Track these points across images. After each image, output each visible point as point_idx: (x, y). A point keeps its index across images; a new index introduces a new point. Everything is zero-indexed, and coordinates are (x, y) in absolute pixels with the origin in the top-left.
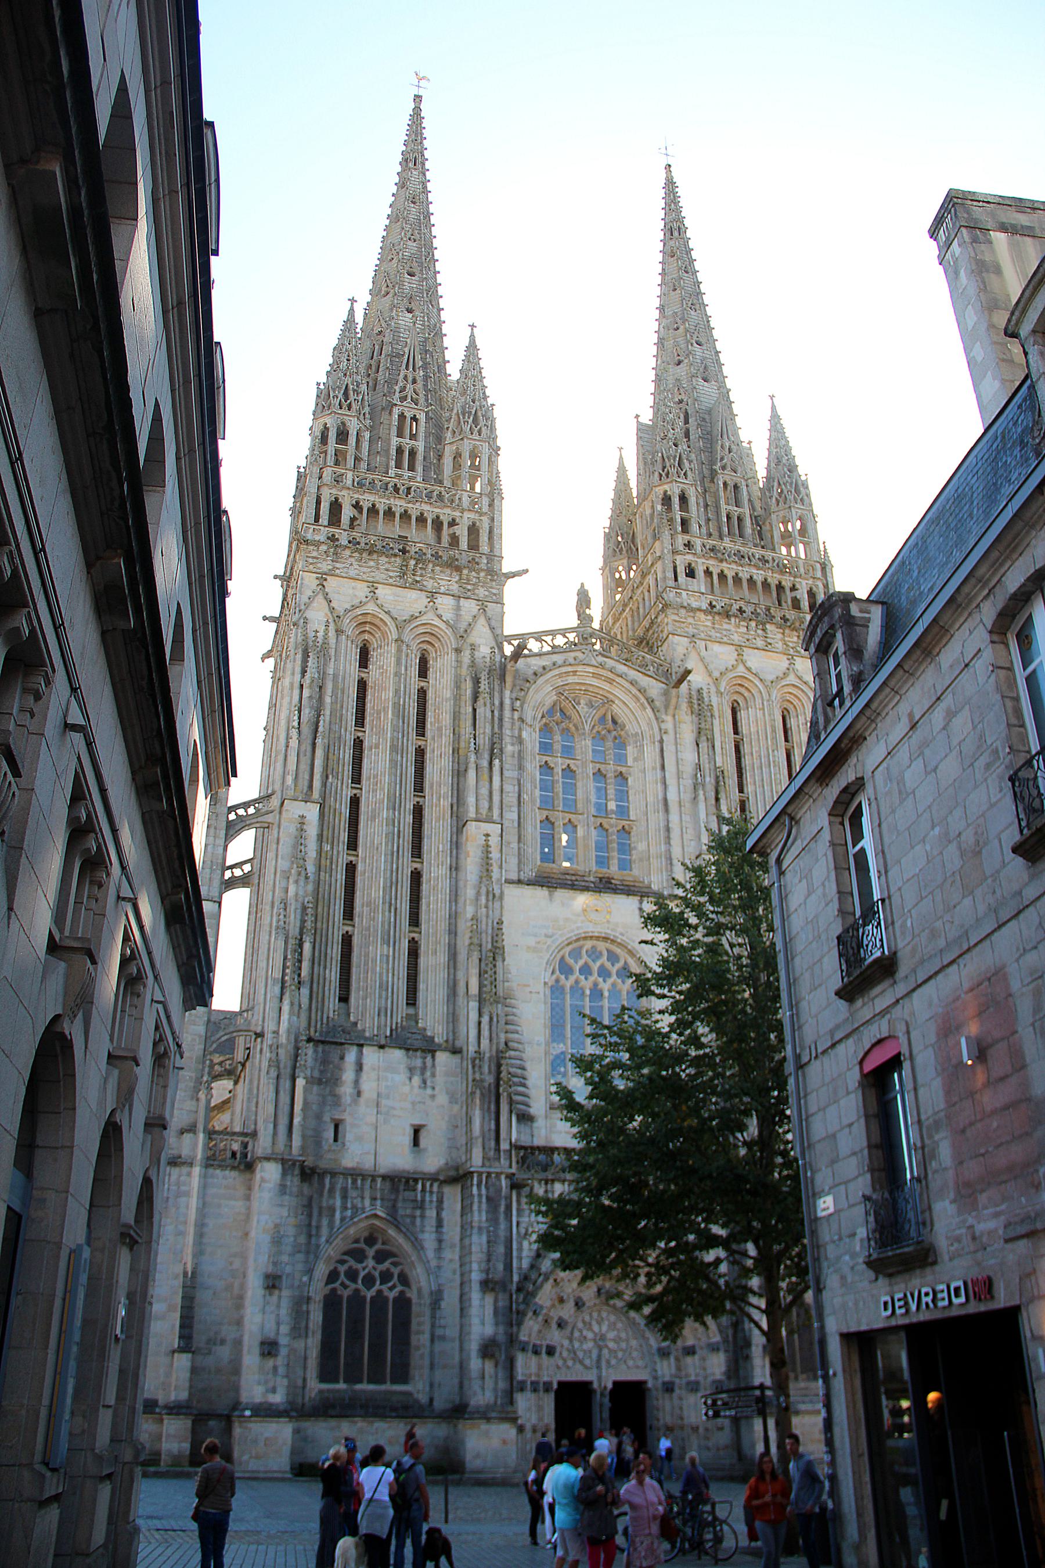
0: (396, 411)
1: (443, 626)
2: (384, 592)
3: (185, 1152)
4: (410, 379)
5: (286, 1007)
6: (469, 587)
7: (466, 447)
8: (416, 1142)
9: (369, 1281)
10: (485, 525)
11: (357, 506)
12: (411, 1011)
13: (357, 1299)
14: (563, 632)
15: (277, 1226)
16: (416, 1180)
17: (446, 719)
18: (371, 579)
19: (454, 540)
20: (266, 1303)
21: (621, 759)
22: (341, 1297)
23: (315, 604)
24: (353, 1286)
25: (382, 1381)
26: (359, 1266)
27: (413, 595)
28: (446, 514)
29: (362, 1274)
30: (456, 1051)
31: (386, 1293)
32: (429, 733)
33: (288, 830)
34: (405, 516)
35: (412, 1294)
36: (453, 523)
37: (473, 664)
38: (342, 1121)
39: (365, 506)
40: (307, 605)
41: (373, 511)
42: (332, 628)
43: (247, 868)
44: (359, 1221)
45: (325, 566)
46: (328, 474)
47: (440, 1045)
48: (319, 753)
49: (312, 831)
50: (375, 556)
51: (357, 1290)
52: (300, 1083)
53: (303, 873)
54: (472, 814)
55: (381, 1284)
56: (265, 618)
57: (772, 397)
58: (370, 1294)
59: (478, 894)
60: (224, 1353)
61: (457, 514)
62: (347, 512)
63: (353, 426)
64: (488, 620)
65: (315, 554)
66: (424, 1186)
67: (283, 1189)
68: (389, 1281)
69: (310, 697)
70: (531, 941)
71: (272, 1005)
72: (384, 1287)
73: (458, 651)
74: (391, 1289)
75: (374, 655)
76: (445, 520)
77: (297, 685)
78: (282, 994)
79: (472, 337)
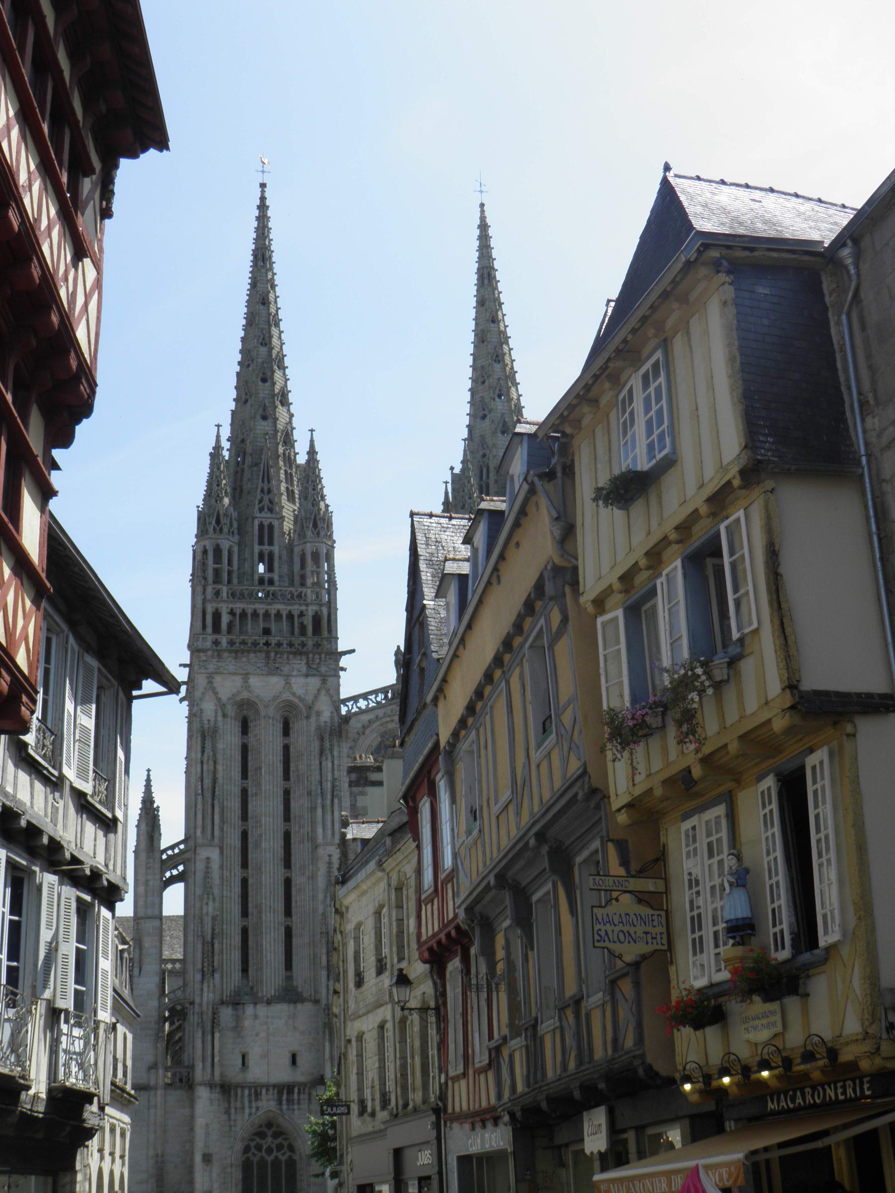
0: (256, 522)
2: (254, 681)
3: (152, 1083)
4: (266, 491)
5: (205, 989)
7: (309, 548)
9: (269, 1151)
10: (325, 611)
11: (232, 613)
12: (289, 974)
13: (262, 1163)
14: (384, 690)
15: (207, 1125)
16: (294, 1087)
18: (244, 672)
19: (303, 628)
23: (207, 697)
24: (259, 1154)
26: (263, 1142)
27: (274, 680)
28: (296, 609)
29: (265, 1147)
30: (317, 1002)
31: (280, 1157)
32: (292, 779)
33: (200, 866)
34: (267, 615)
35: (296, 1157)
36: (302, 614)
37: (318, 728)
39: (238, 612)
40: (201, 699)
41: (243, 614)
42: (220, 713)
45: (212, 667)
46: (210, 590)
48: (217, 810)
49: (215, 866)
50: (246, 654)
51: (262, 1158)
52: (217, 1035)
53: (211, 897)
54: (320, 840)
58: (270, 1159)
59: (325, 897)
61: (303, 608)
62: (225, 619)
63: (225, 545)
64: (328, 690)
65: (204, 658)
66: (299, 1089)
69: (208, 770)
71: (198, 986)
72: (279, 1155)
73: (308, 717)
74: (283, 1154)
75: (251, 724)
77: (199, 761)
78: (203, 979)
79: (312, 442)
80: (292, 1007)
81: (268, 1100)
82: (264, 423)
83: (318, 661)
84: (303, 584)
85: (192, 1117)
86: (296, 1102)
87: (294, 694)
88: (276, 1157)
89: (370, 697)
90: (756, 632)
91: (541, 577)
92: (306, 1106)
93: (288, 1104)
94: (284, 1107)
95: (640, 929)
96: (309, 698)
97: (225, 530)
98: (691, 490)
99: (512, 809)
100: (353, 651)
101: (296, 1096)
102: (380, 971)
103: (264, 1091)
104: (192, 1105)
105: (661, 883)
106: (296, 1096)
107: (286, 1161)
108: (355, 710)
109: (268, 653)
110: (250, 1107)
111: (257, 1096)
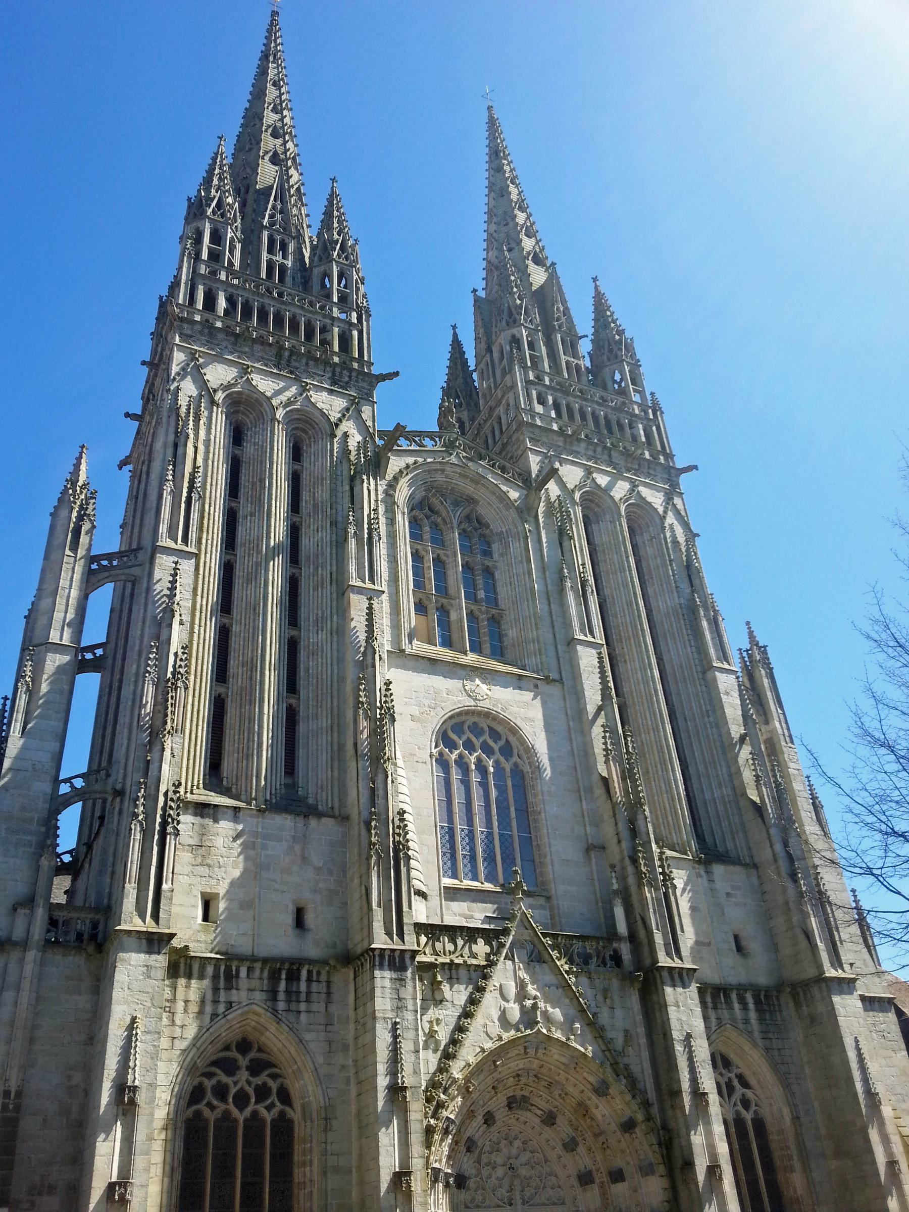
10: (355, 333)
11: (231, 300)
14: (431, 436)
21: (487, 553)
22: (207, 1121)
24: (222, 1106)
29: (233, 1091)
31: (263, 1112)
35: (295, 1115)
43: (99, 652)
51: (227, 1114)
55: (257, 1102)
56: (127, 415)
57: (595, 280)
58: (241, 1117)
65: (189, 332)
66: (310, 972)
68: (266, 1098)
70: (416, 711)
74: (269, 1108)
80: (300, 820)
81: (251, 990)
83: (347, 379)
86: (303, 996)
88: (255, 1113)
92: (323, 1005)
93: (288, 1001)
94: (281, 1005)
100: (396, 374)
101: (303, 987)
106: (303, 987)
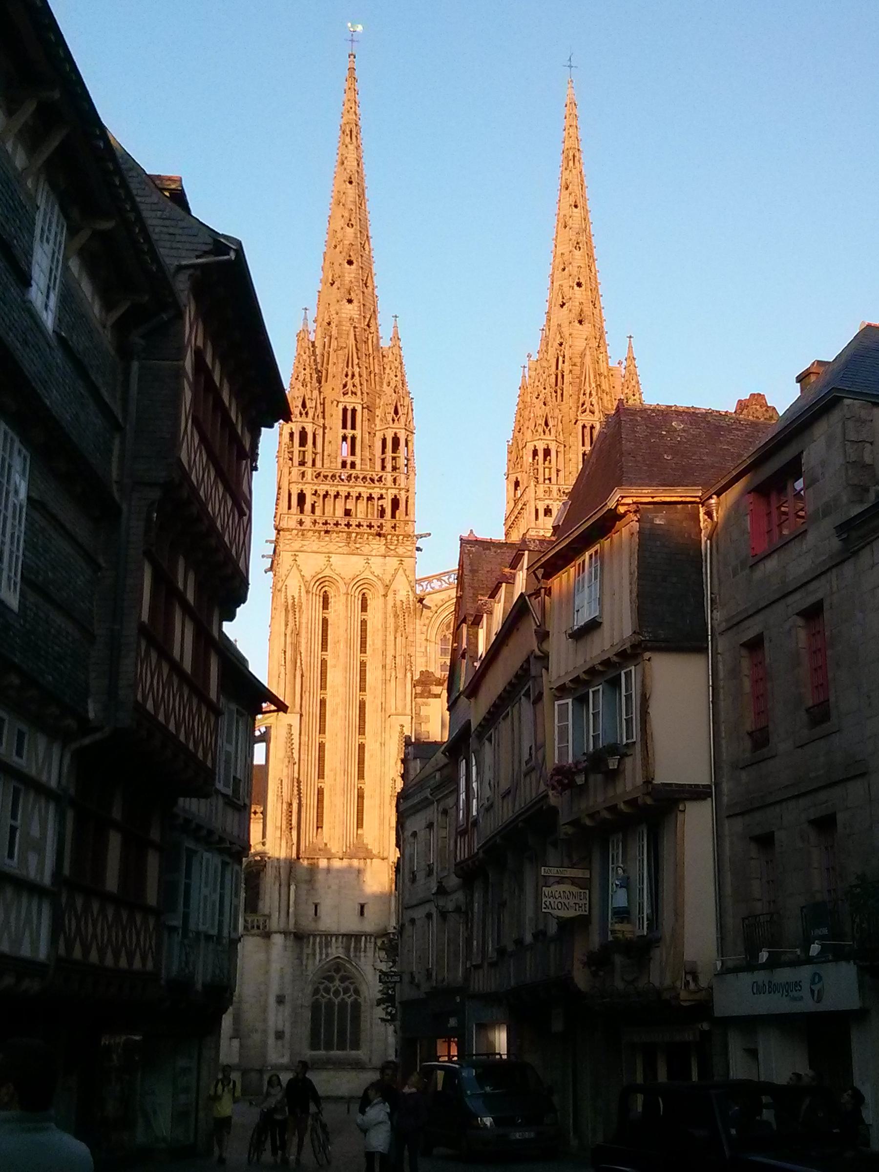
1: (375, 579)
6: (392, 547)
8: (362, 913)
15: (282, 968)
17: (379, 644)
18: (327, 551)
20: (277, 1011)
24: (329, 997)
25: (344, 1049)
26: (331, 985)
27: (354, 558)
36: (381, 497)
38: (318, 903)
40: (287, 576)
44: (331, 960)
45: (297, 545)
47: (374, 855)
49: (295, 731)
52: (293, 888)
55: (344, 994)
58: (336, 1001)
60: (257, 1037)
61: (384, 491)
65: (290, 537)
67: (285, 948)
72: (345, 997)
73: (385, 596)
74: (349, 997)
75: (331, 600)
76: (375, 496)
79: (395, 327)
82: (350, 306)
84: (383, 468)
85: (268, 961)
87: (373, 573)
88: (343, 999)
89: (443, 578)
90: (634, 743)
91: (528, 661)
95: (572, 901)
96: (387, 578)
97: (311, 414)
98: (607, 647)
99: (510, 797)
100: (430, 534)
102: (430, 873)
103: (334, 939)
104: (268, 951)
105: (588, 872)
107: (351, 1003)
108: (429, 589)
109: (349, 533)
110: (321, 954)
111: (328, 945)
